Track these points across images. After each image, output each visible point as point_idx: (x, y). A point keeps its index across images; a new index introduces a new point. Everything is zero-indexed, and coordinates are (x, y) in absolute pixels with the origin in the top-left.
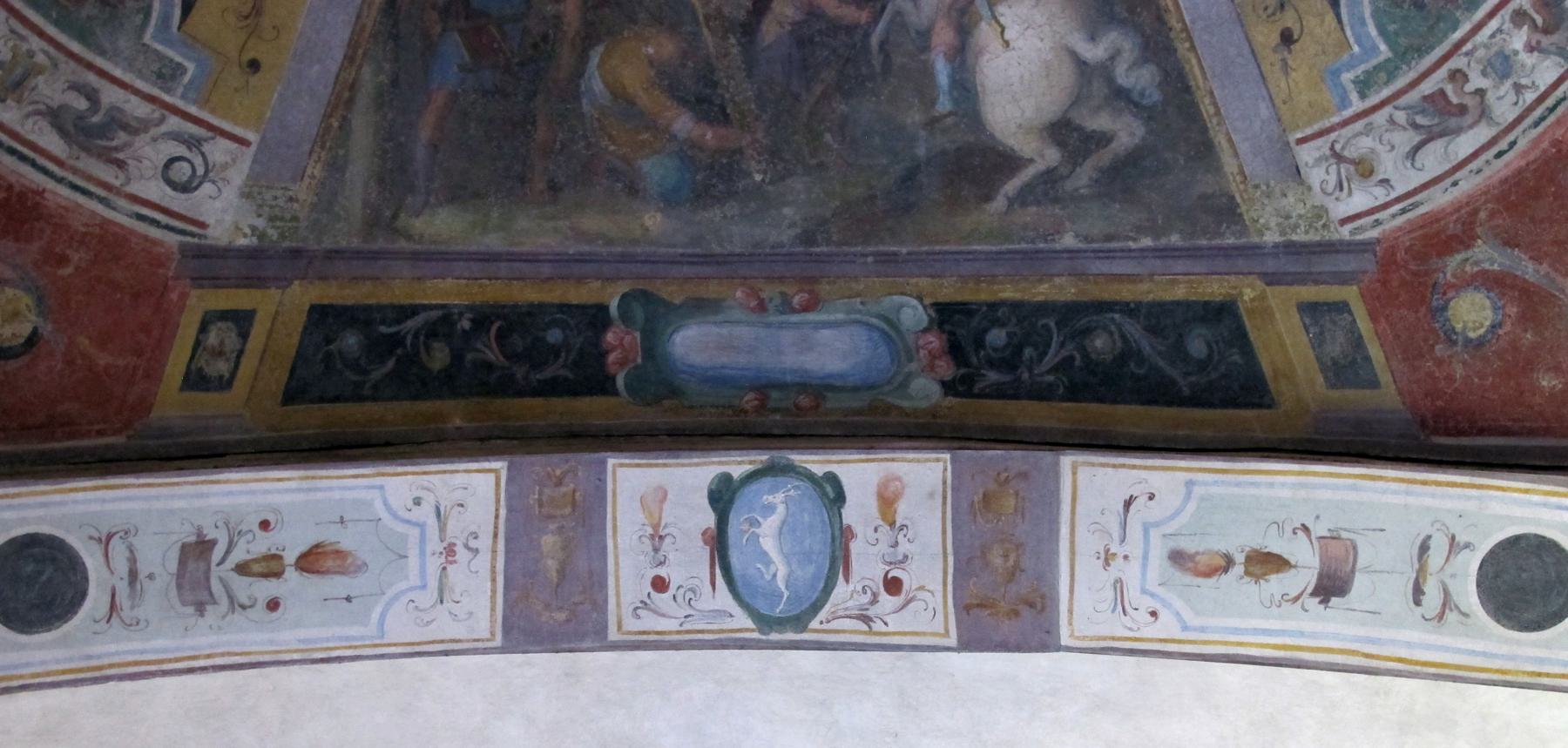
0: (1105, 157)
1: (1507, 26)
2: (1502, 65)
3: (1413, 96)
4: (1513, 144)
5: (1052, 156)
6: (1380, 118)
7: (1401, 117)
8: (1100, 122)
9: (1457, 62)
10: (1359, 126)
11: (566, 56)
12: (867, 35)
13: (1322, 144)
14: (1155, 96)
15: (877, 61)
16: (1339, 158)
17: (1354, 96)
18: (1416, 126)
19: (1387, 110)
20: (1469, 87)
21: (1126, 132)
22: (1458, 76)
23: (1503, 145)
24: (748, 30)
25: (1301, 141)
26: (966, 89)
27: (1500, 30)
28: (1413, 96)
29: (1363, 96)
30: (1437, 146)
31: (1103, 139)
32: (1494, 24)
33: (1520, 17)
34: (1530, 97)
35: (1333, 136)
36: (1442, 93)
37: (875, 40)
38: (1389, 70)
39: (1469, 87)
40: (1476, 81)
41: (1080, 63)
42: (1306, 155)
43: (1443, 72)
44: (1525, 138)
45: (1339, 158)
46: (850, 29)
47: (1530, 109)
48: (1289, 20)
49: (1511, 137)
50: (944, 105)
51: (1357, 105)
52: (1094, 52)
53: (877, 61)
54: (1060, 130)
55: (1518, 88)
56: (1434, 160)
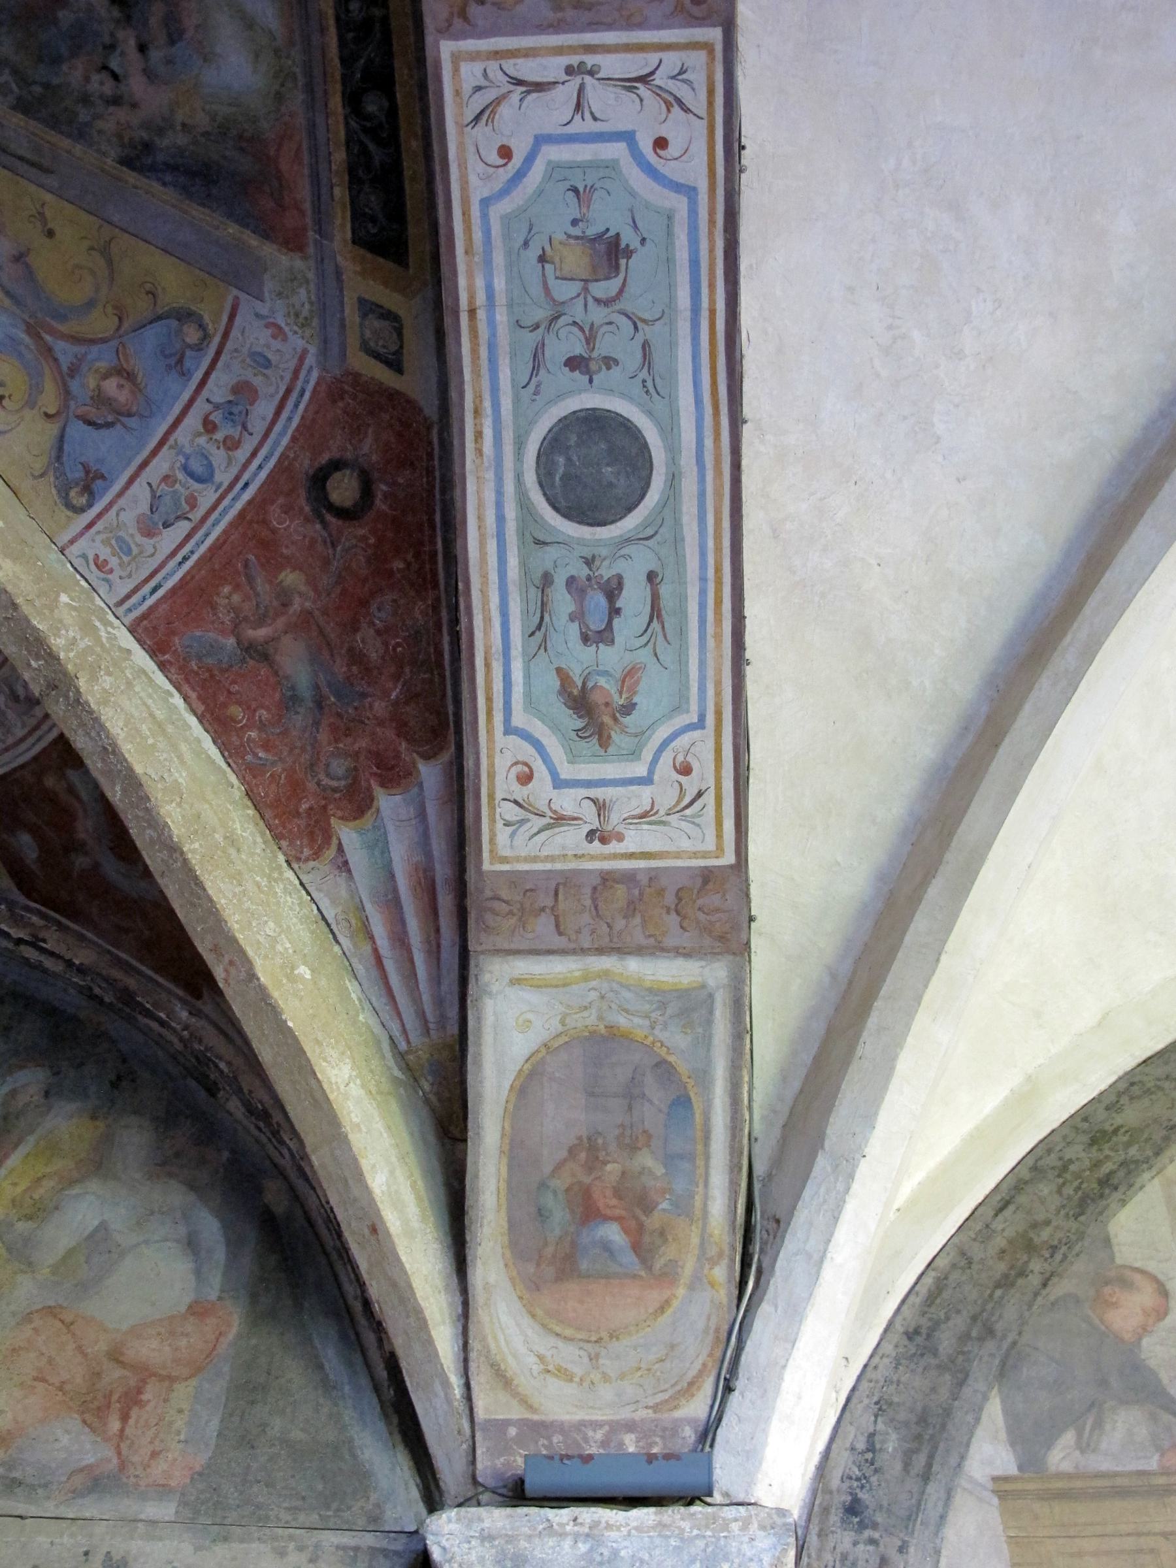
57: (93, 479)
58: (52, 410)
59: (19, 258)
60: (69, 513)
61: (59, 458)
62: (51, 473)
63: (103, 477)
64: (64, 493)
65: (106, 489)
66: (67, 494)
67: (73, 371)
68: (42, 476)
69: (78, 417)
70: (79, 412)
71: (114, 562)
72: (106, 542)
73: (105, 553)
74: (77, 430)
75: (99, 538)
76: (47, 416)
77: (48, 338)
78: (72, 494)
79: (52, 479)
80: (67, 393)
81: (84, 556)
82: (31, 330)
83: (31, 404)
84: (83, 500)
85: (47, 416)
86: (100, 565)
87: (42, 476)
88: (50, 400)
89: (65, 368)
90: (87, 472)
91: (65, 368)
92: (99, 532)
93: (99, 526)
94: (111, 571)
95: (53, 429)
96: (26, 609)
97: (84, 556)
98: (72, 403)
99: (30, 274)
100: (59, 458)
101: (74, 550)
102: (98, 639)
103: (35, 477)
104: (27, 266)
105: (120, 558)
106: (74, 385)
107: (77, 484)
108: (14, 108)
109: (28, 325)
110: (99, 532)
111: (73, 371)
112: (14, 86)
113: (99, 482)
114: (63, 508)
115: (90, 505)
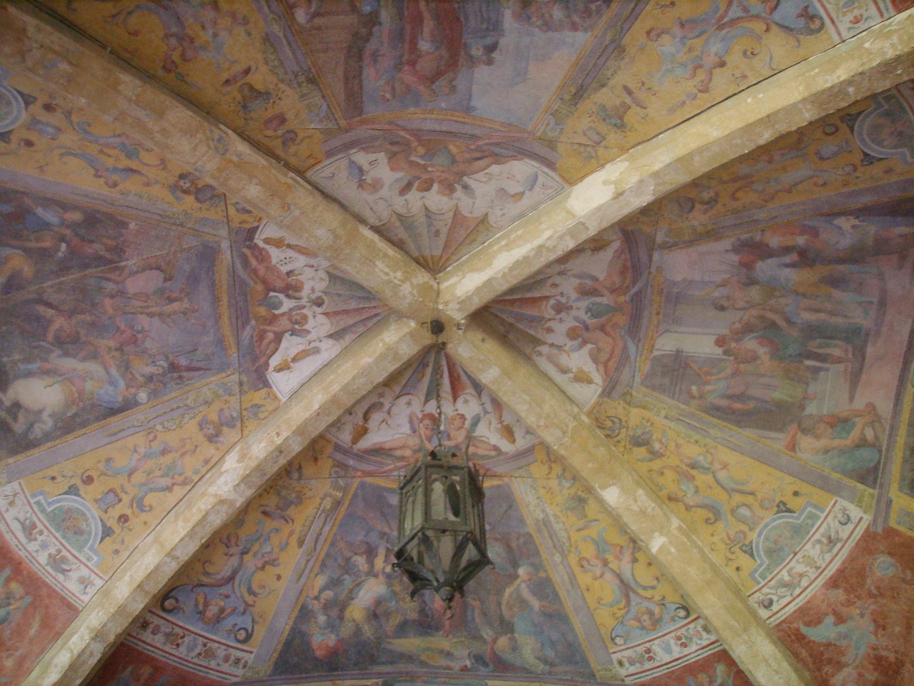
0: (9, 420)
1: (56, 548)
2: (44, 546)
3: (35, 519)
4: (20, 550)
5: (8, 403)
6: (28, 508)
7: (28, 515)
8: (21, 417)
9: (46, 532)
10: (26, 502)
11: (16, 243)
12: (43, 341)
13: (18, 490)
14: (32, 437)
15: (34, 344)
16: (15, 495)
17: (36, 499)
18: (26, 519)
19: (31, 511)
20: (38, 536)
21: (19, 427)
22: (41, 533)
23: (20, 547)
24: (40, 301)
25: (20, 484)
26: (29, 374)
27: (55, 545)
28: (35, 519)
29: (35, 503)
30: (19, 526)
31: (15, 419)
32: (57, 543)
33: (59, 551)
34: (34, 554)
35: (22, 493)
36: (36, 527)
37: (42, 343)
38: (43, 511)
39: (38, 536)
40: (40, 538)
41: (40, 412)
42: (15, 485)
43: (42, 528)
44: (22, 553)
45: (15, 495)
46: (45, 335)
47: (30, 554)
48: (60, 479)
49: (23, 549)
50: (22, 367)
51: (32, 501)
52: (45, 416)
53: (34, 344)
54: (17, 406)
55: (37, 551)
56: (16, 527)
57: (807, 13)
58: (765, 27)
59: (682, 25)
60: (822, 32)
61: (791, 30)
62: (798, 36)
63: (807, 7)
64: (812, 32)
65: (815, 8)
66: (812, 30)
67: (746, 10)
68: (799, 41)
69: (771, 13)
70: (768, 11)
71: (856, 12)
72: (844, 14)
73: (850, 17)
74: (776, 16)
75: (841, 18)
76: (767, 30)
77: (725, 20)
78: (812, 27)
79: (802, 37)
80: (757, 17)
81: (849, 29)
82: (721, 27)
83: (759, 38)
84: (817, 23)
85: (767, 30)
86: (857, 21)
87: (799, 41)
88: (759, 27)
89: (744, 15)
90: (802, 15)
91: (744, 15)
92: (838, 17)
93: (834, 16)
94: (861, 15)
95: (775, 29)
96: (867, 67)
97: (849, 29)
98: (764, 15)
99: (693, 22)
100: (791, 30)
101: (845, 34)
102: (895, 31)
103: (798, 46)
104: (686, 21)
105: (854, 8)
106: (754, 11)
107: (808, 23)
108: (608, 6)
109: (717, 29)
110: (838, 17)
111: (746, 10)
112: (598, 3)
113: (810, 10)
114: (819, 35)
115: (821, 19)
